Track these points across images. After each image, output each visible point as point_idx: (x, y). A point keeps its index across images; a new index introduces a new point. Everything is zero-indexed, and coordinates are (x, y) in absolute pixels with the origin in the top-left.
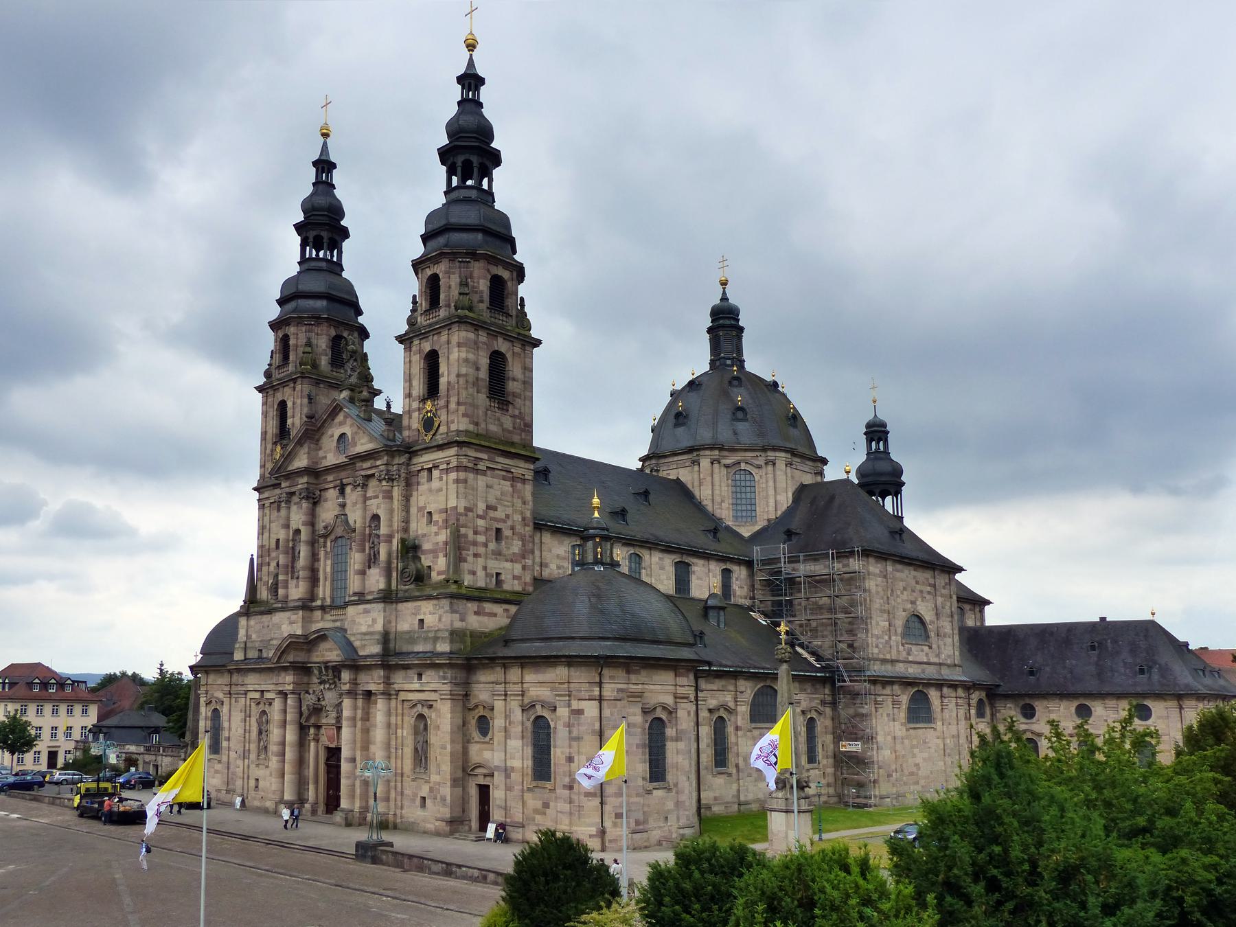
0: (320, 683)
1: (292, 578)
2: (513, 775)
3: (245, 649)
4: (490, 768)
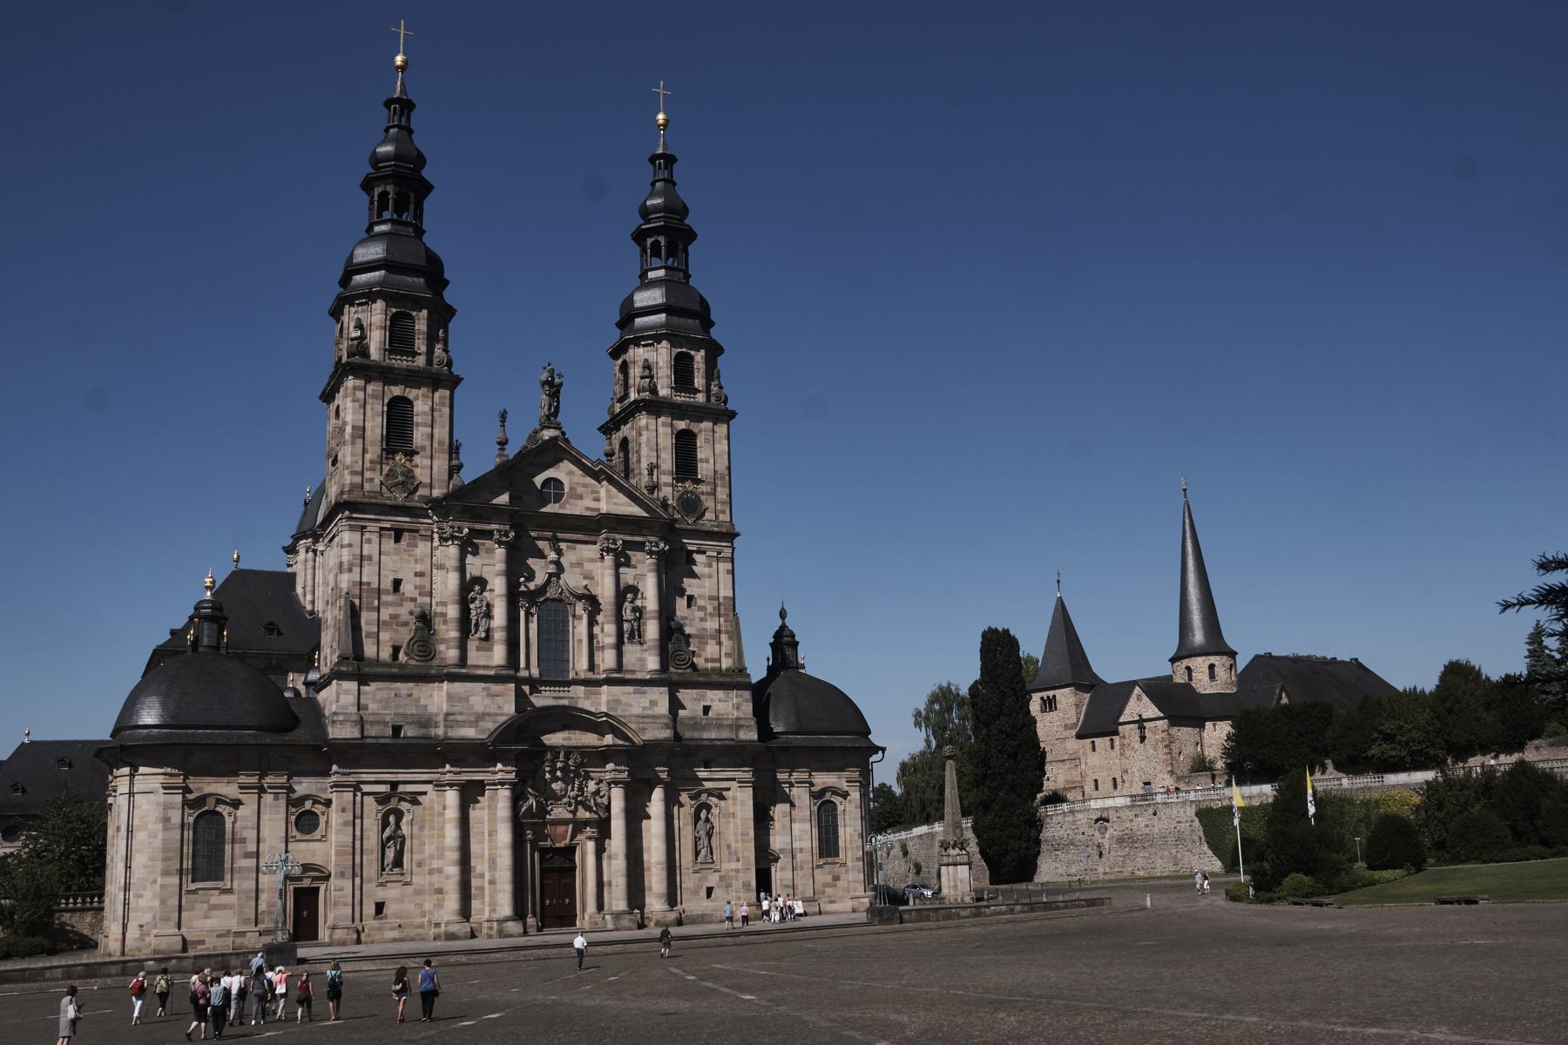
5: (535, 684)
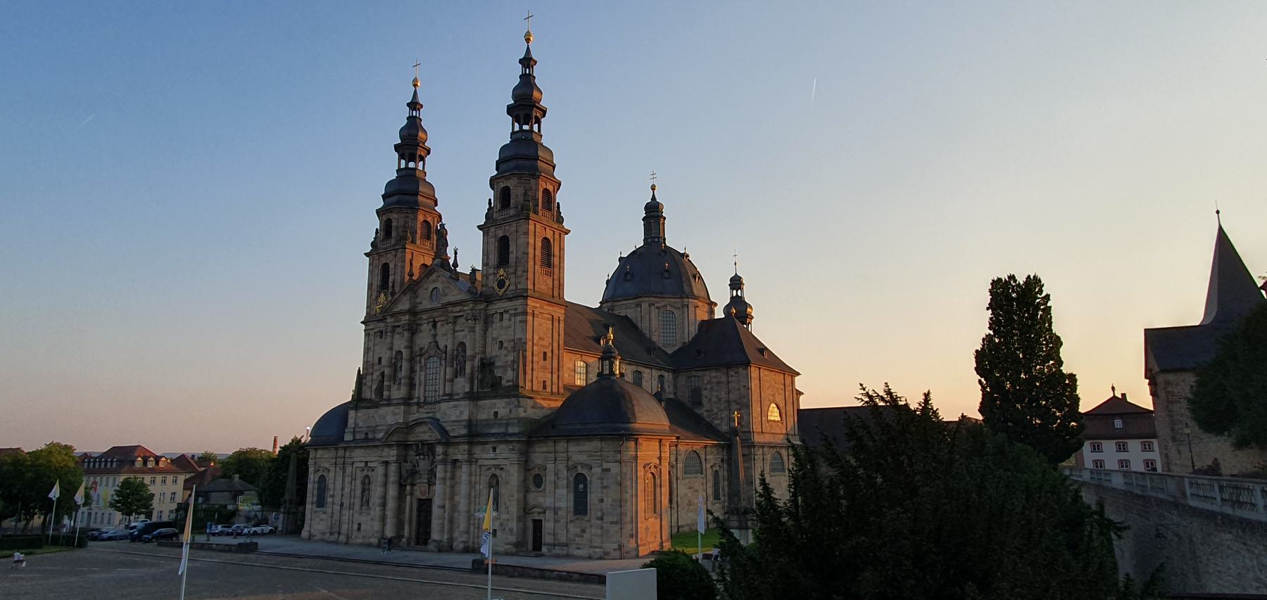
0: (417, 455)
2: (560, 512)
4: (543, 508)
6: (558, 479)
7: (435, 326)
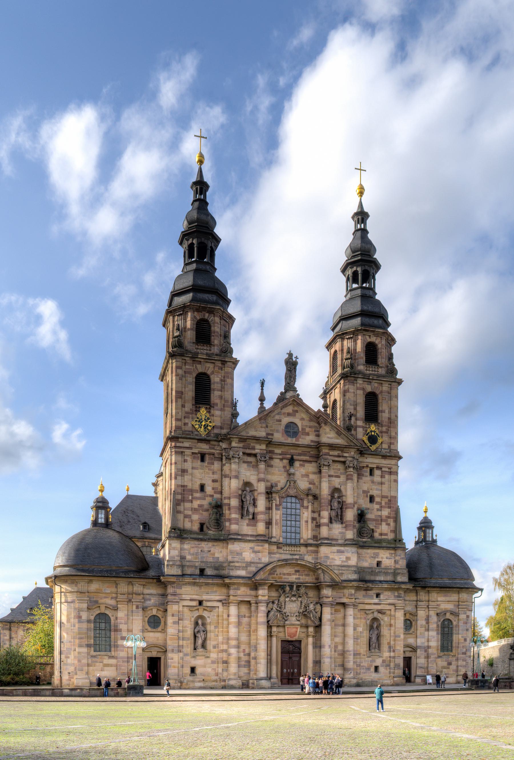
1: (242, 518)
3: (182, 566)
5: (279, 545)
6: (428, 623)
7: (292, 461)
